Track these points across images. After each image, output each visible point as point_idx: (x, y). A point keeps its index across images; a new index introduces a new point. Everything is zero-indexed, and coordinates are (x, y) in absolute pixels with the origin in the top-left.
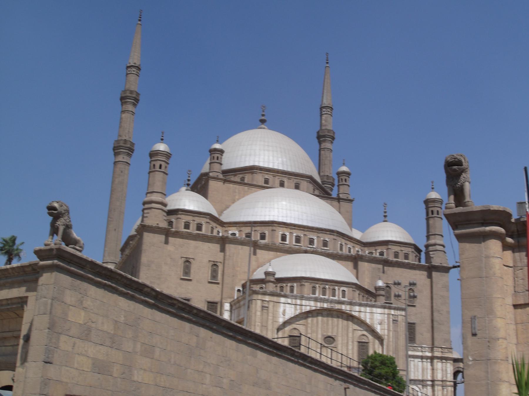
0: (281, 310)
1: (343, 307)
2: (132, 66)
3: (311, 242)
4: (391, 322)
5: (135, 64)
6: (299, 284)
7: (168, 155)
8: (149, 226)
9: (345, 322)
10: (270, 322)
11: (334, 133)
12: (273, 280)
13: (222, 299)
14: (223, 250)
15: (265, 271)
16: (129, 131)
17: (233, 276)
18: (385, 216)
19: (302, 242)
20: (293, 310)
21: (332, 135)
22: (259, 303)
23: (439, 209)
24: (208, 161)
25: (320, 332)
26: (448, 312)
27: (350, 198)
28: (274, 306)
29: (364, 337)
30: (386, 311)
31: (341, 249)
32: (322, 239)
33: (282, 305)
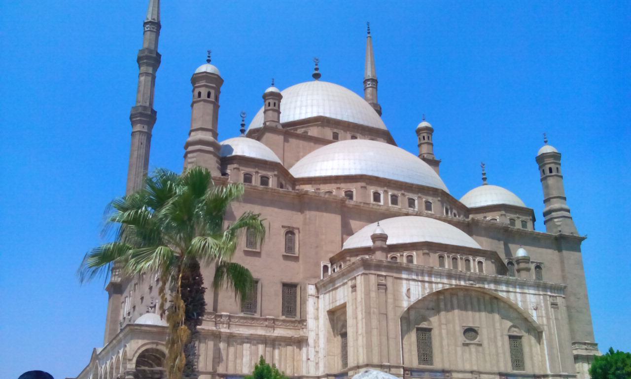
2: (150, 22)
3: (411, 203)
4: (549, 306)
5: (154, 19)
10: (390, 307)
11: (381, 108)
12: (385, 246)
15: (372, 234)
17: (317, 247)
18: (484, 179)
20: (420, 289)
21: (379, 109)
23: (558, 166)
24: (263, 109)
26: (586, 296)
27: (436, 159)
28: (393, 284)
29: (515, 329)
31: (447, 212)
32: (424, 200)
33: (404, 282)
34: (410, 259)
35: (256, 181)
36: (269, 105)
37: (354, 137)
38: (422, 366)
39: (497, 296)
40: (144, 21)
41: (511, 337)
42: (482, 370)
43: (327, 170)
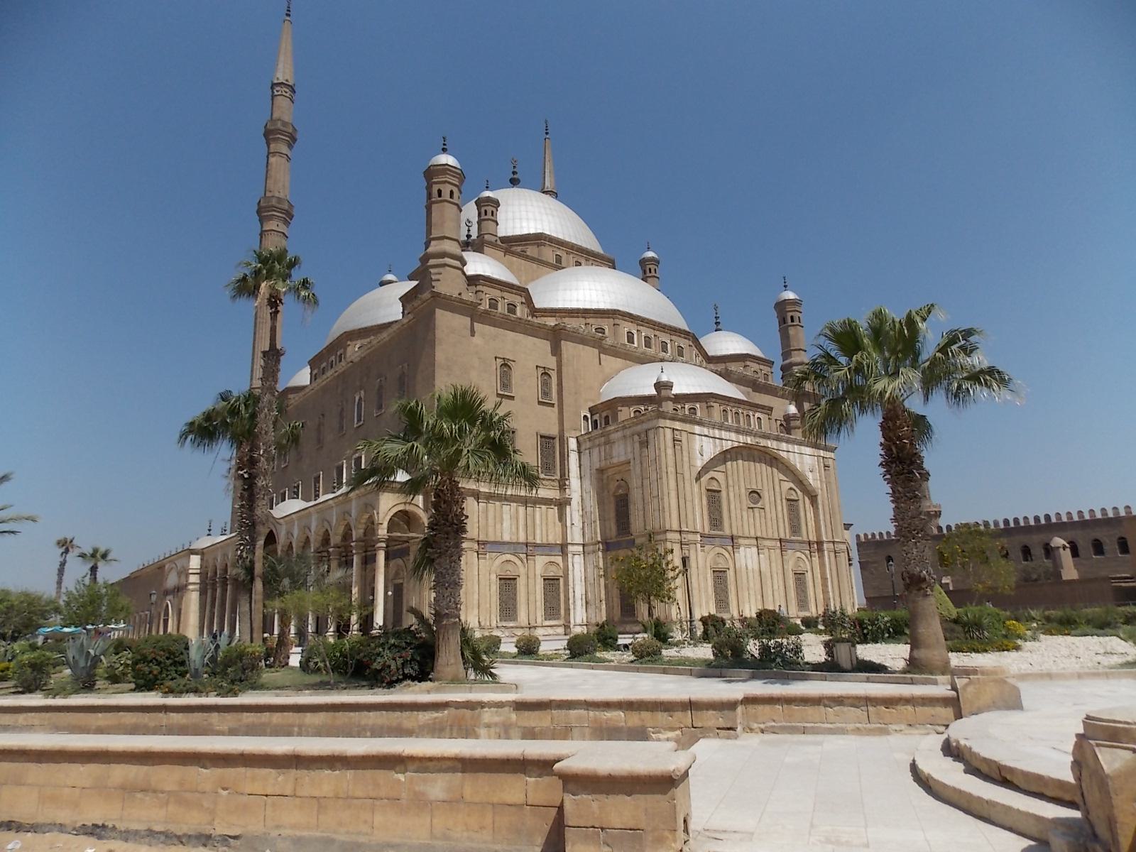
0: (697, 447)
1: (769, 443)
2: (282, 83)
3: (664, 349)
5: (287, 81)
6: (704, 405)
7: (461, 176)
8: (446, 297)
9: (769, 468)
13: (562, 431)
14: (556, 351)
16: (284, 186)
17: (576, 393)
19: (653, 347)
20: (712, 445)
22: (668, 432)
25: (742, 484)
29: (793, 492)
30: (816, 452)
33: (697, 436)
34: (693, 410)
35: (502, 308)
36: (486, 214)
37: (578, 264)
38: (713, 532)
39: (778, 457)
40: (272, 82)
41: (788, 500)
42: (765, 536)
43: (571, 301)
